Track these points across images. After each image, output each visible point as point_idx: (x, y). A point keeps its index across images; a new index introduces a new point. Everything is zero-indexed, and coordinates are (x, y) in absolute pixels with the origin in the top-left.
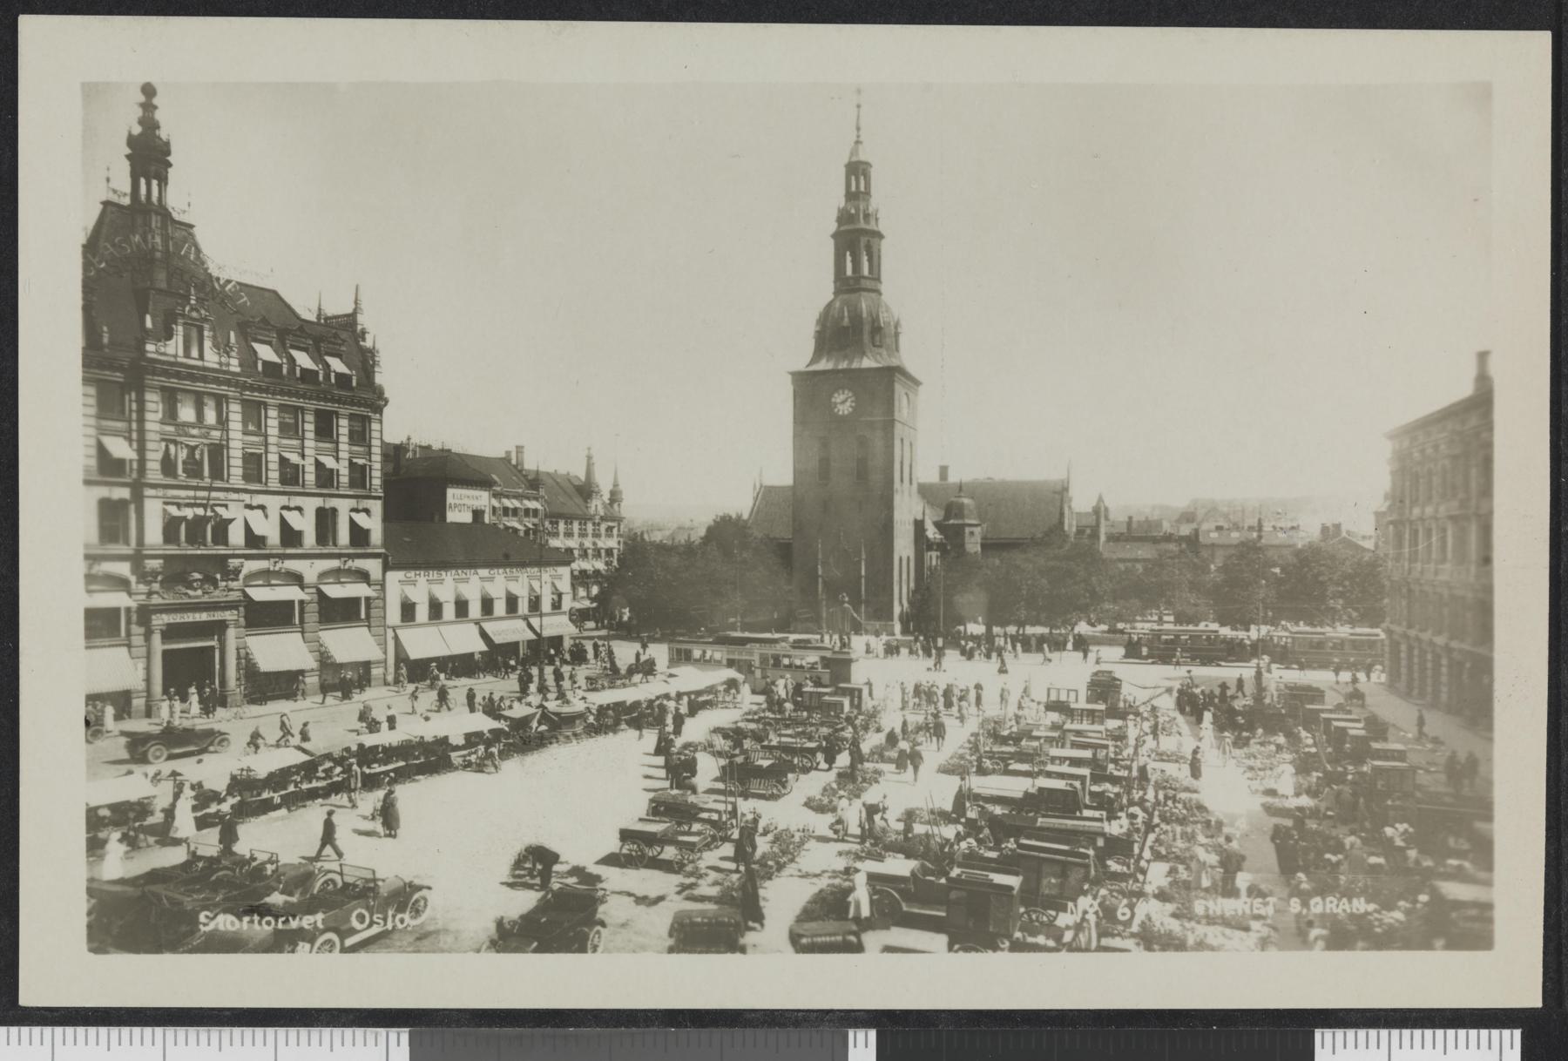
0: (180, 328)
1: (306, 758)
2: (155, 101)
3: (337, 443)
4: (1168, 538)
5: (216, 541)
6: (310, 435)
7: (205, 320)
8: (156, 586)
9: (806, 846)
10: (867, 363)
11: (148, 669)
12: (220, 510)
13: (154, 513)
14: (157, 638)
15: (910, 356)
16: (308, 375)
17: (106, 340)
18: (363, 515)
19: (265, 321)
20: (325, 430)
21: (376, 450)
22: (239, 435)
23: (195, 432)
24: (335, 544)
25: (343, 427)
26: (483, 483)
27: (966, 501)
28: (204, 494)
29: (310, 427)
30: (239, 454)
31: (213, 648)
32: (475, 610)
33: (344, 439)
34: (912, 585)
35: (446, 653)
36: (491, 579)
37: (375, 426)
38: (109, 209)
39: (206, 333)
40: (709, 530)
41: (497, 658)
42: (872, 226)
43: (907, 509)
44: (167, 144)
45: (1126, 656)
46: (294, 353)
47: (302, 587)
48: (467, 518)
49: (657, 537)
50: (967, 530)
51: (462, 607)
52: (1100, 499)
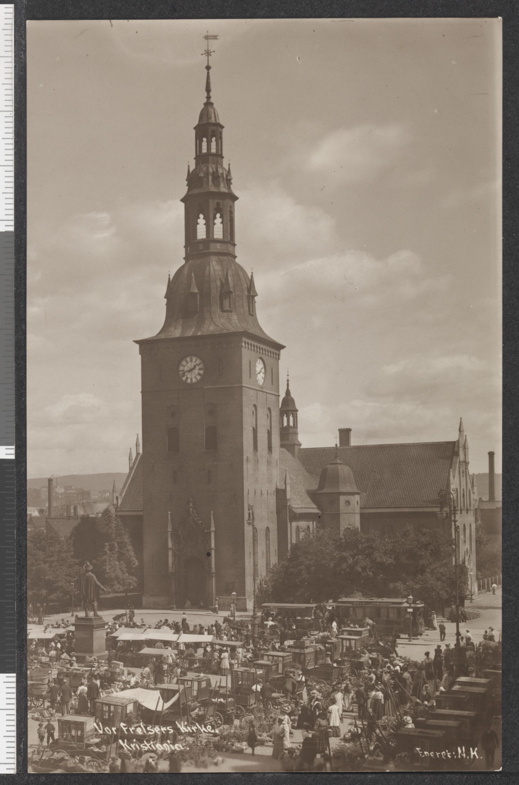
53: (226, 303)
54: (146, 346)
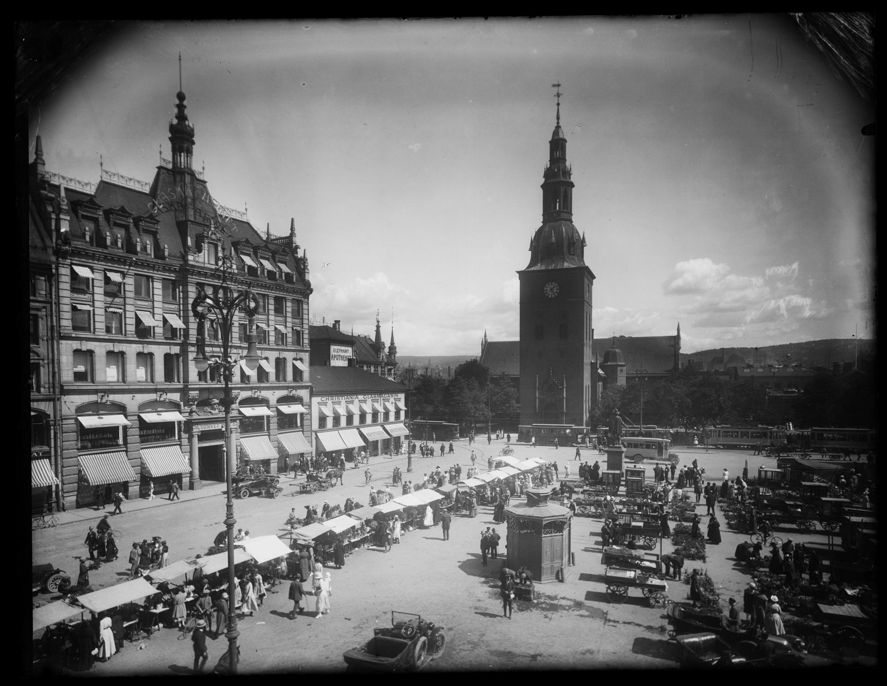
0: (206, 245)
2: (185, 103)
6: (272, 312)
7: (219, 240)
8: (194, 407)
10: (566, 265)
11: (191, 460)
14: (195, 439)
16: (271, 274)
17: (166, 254)
19: (247, 241)
20: (279, 310)
25: (289, 307)
29: (272, 307)
31: (221, 446)
32: (356, 421)
33: (289, 315)
36: (365, 401)
37: (305, 306)
38: (162, 171)
44: (193, 130)
46: (263, 261)
47: (269, 407)
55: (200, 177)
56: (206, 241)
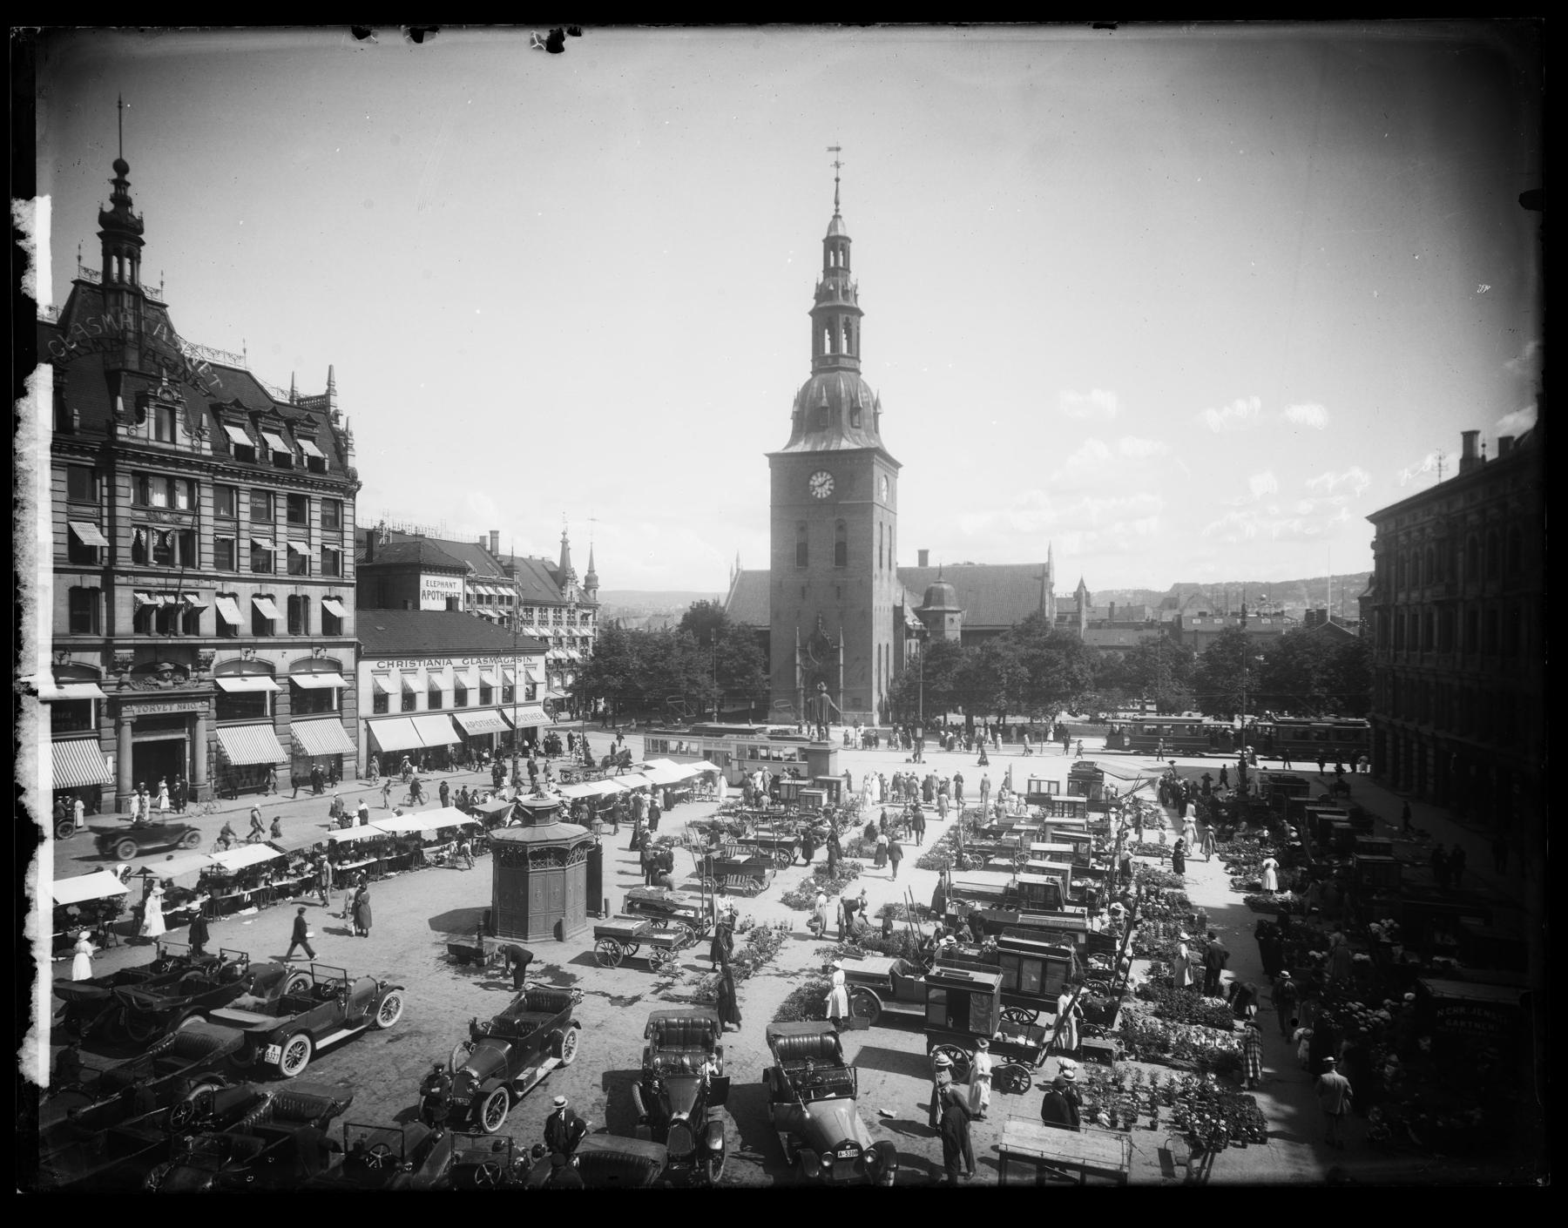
0: (152, 411)
1: (277, 854)
2: (128, 178)
3: (342, 532)
4: (1150, 625)
5: (187, 631)
6: (282, 520)
7: (178, 402)
8: (126, 677)
9: (784, 944)
10: (845, 444)
11: (118, 763)
12: (191, 598)
13: (124, 602)
14: (127, 730)
15: (892, 435)
16: (281, 459)
17: (76, 424)
18: (336, 602)
19: (237, 403)
20: (297, 515)
21: (349, 536)
22: (211, 521)
23: (166, 517)
24: (307, 633)
25: (316, 511)
26: (459, 570)
27: (945, 587)
28: (175, 581)
29: (282, 512)
30: (210, 540)
31: (183, 741)
32: (448, 701)
33: (316, 524)
34: (891, 674)
35: (420, 745)
37: (348, 511)
38: (81, 287)
39: (178, 416)
40: (685, 617)
41: (470, 749)
42: (851, 303)
43: (886, 595)
44: (140, 221)
45: (1108, 747)
46: (267, 436)
47: (274, 678)
48: (441, 605)
49: (633, 625)
50: (947, 616)
51: (435, 698)
52: (1082, 585)
53: (856, 418)
54: (775, 459)
55: (157, 298)
56: (152, 403)
